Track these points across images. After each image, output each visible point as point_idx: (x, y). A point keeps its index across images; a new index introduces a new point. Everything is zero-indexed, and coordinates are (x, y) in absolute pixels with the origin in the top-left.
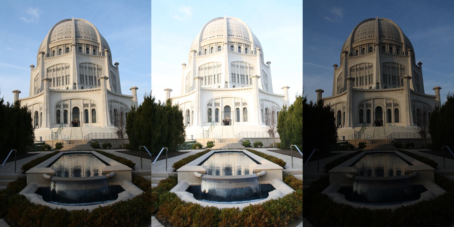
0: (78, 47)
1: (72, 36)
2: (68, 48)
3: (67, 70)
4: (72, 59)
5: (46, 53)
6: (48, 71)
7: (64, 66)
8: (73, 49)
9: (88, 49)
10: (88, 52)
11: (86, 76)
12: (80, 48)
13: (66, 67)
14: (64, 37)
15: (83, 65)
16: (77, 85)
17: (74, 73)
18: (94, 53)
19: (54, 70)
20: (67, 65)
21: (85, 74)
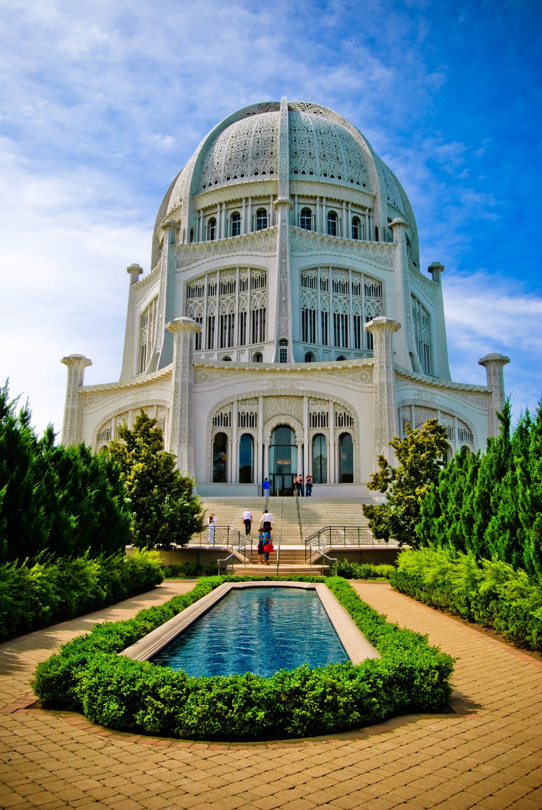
0: (298, 209)
1: (278, 168)
2: (262, 213)
3: (259, 291)
4: (277, 253)
5: (185, 226)
6: (191, 291)
7: (247, 275)
8: (279, 218)
9: (332, 216)
10: (332, 230)
11: (325, 316)
12: (306, 212)
13: (252, 279)
14: (249, 170)
15: (312, 274)
16: (290, 348)
17: (282, 304)
18: (355, 230)
19: (211, 290)
20: (257, 275)
21: (319, 308)
